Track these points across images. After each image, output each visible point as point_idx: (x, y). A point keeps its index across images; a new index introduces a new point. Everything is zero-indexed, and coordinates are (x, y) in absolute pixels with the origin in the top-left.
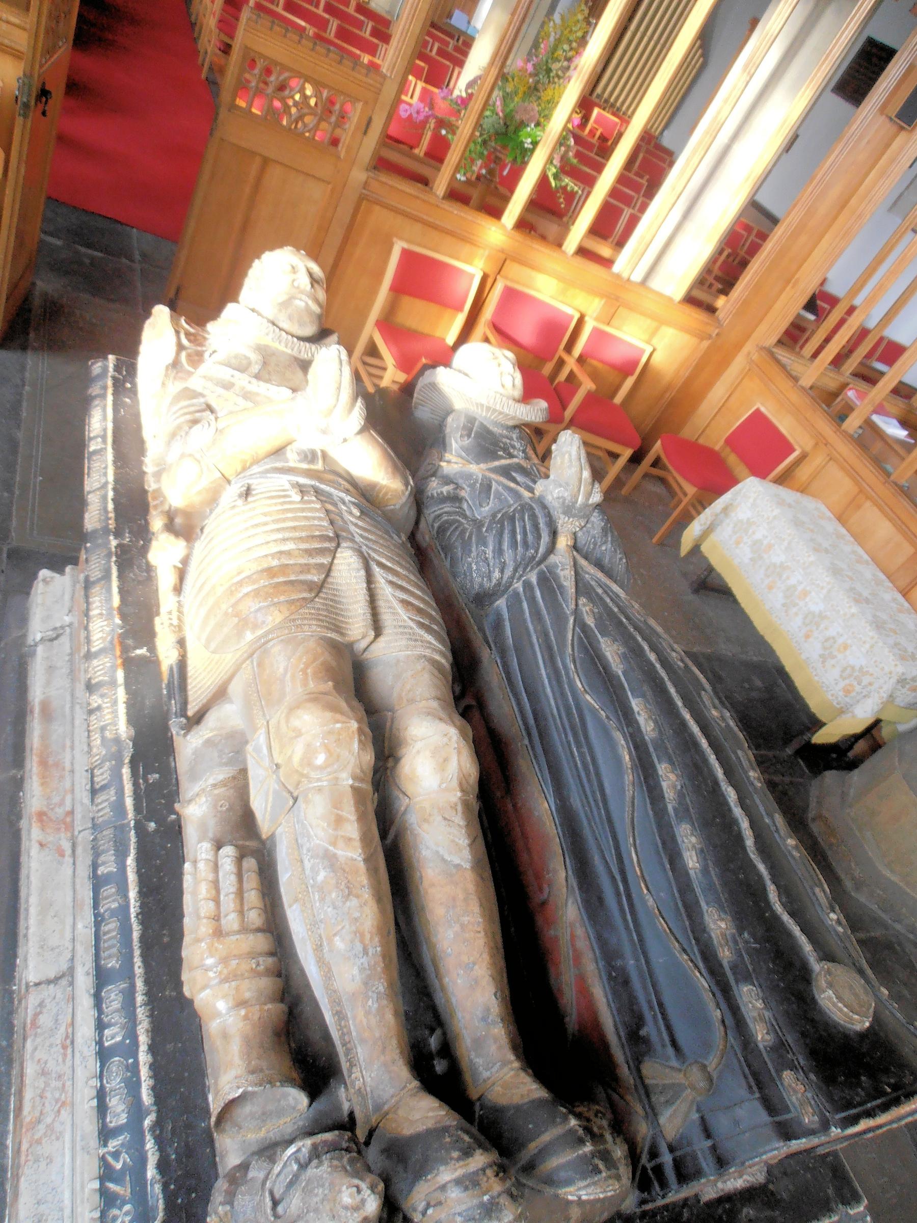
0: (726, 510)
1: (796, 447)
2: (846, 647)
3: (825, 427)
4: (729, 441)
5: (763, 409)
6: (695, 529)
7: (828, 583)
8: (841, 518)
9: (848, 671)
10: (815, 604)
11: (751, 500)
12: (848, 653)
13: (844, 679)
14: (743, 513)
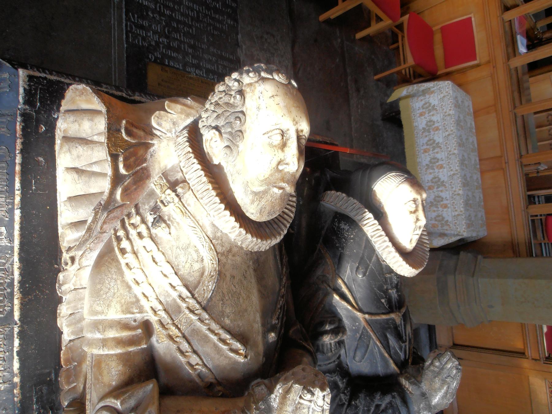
0: (424, 92)
1: (478, 58)
2: (446, 206)
3: (500, 53)
4: (443, 29)
5: (473, 19)
6: (403, 91)
7: (457, 170)
8: (476, 113)
9: (440, 218)
10: (443, 174)
11: (442, 95)
12: (445, 210)
13: (436, 220)
14: (434, 100)
